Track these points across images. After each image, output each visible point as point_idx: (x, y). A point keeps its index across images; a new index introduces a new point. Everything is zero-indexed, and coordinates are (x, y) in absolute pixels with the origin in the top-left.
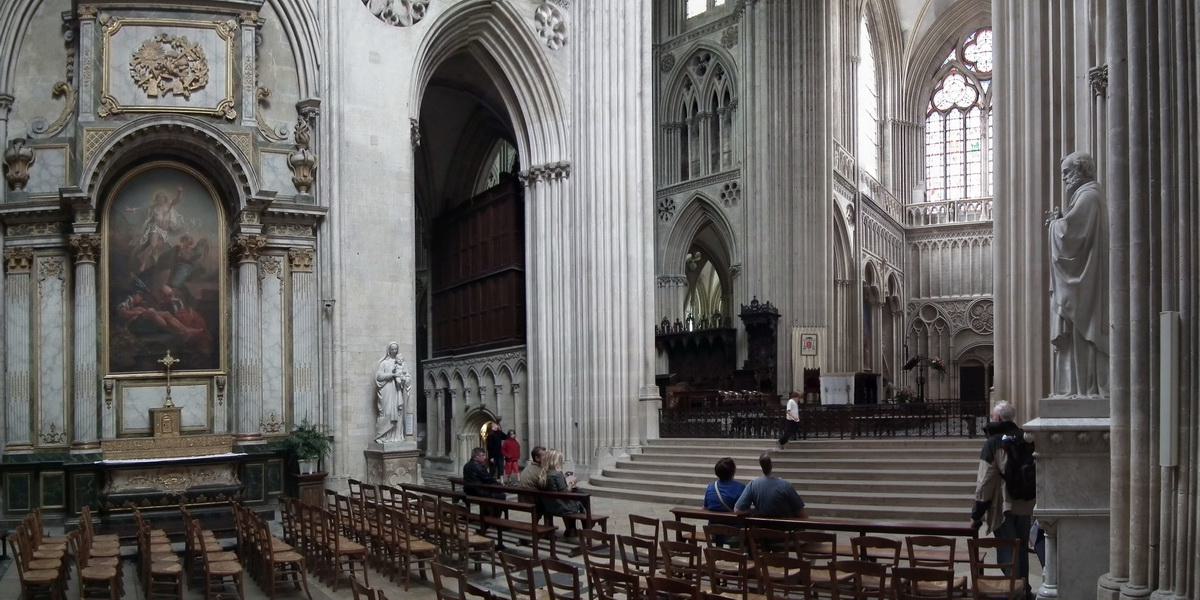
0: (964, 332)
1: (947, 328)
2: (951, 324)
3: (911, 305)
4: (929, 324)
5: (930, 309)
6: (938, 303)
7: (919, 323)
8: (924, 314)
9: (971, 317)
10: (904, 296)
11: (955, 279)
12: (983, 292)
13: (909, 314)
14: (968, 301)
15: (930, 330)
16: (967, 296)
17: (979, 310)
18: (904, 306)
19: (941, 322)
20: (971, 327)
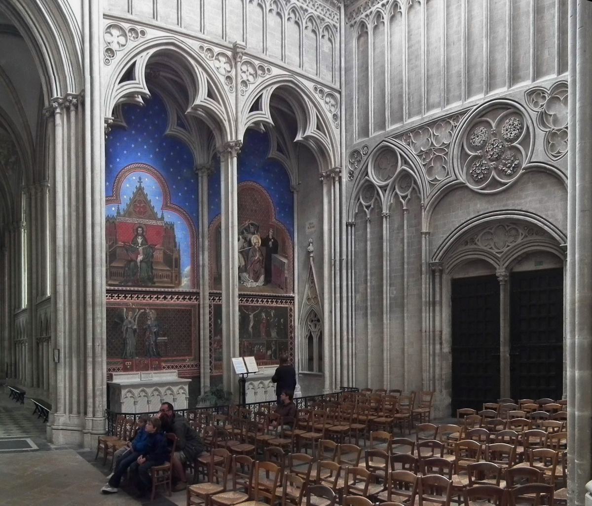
0: (453, 190)
1: (416, 191)
2: (422, 178)
3: (355, 154)
4: (384, 188)
5: (385, 154)
6: (399, 136)
7: (369, 188)
8: (378, 168)
9: (464, 155)
10: (335, 131)
11: (434, 71)
12: (491, 86)
13: (351, 174)
14: (456, 116)
15: (386, 200)
16: (455, 106)
17: (481, 134)
18: (339, 156)
19: (406, 178)
20: (462, 179)
